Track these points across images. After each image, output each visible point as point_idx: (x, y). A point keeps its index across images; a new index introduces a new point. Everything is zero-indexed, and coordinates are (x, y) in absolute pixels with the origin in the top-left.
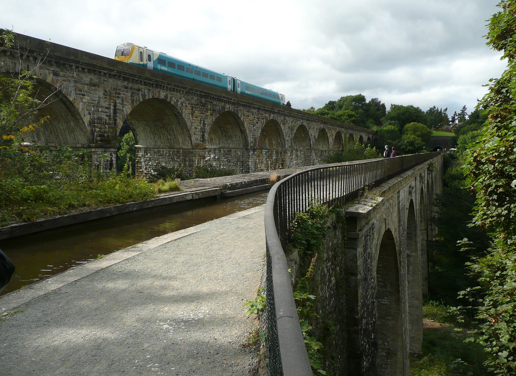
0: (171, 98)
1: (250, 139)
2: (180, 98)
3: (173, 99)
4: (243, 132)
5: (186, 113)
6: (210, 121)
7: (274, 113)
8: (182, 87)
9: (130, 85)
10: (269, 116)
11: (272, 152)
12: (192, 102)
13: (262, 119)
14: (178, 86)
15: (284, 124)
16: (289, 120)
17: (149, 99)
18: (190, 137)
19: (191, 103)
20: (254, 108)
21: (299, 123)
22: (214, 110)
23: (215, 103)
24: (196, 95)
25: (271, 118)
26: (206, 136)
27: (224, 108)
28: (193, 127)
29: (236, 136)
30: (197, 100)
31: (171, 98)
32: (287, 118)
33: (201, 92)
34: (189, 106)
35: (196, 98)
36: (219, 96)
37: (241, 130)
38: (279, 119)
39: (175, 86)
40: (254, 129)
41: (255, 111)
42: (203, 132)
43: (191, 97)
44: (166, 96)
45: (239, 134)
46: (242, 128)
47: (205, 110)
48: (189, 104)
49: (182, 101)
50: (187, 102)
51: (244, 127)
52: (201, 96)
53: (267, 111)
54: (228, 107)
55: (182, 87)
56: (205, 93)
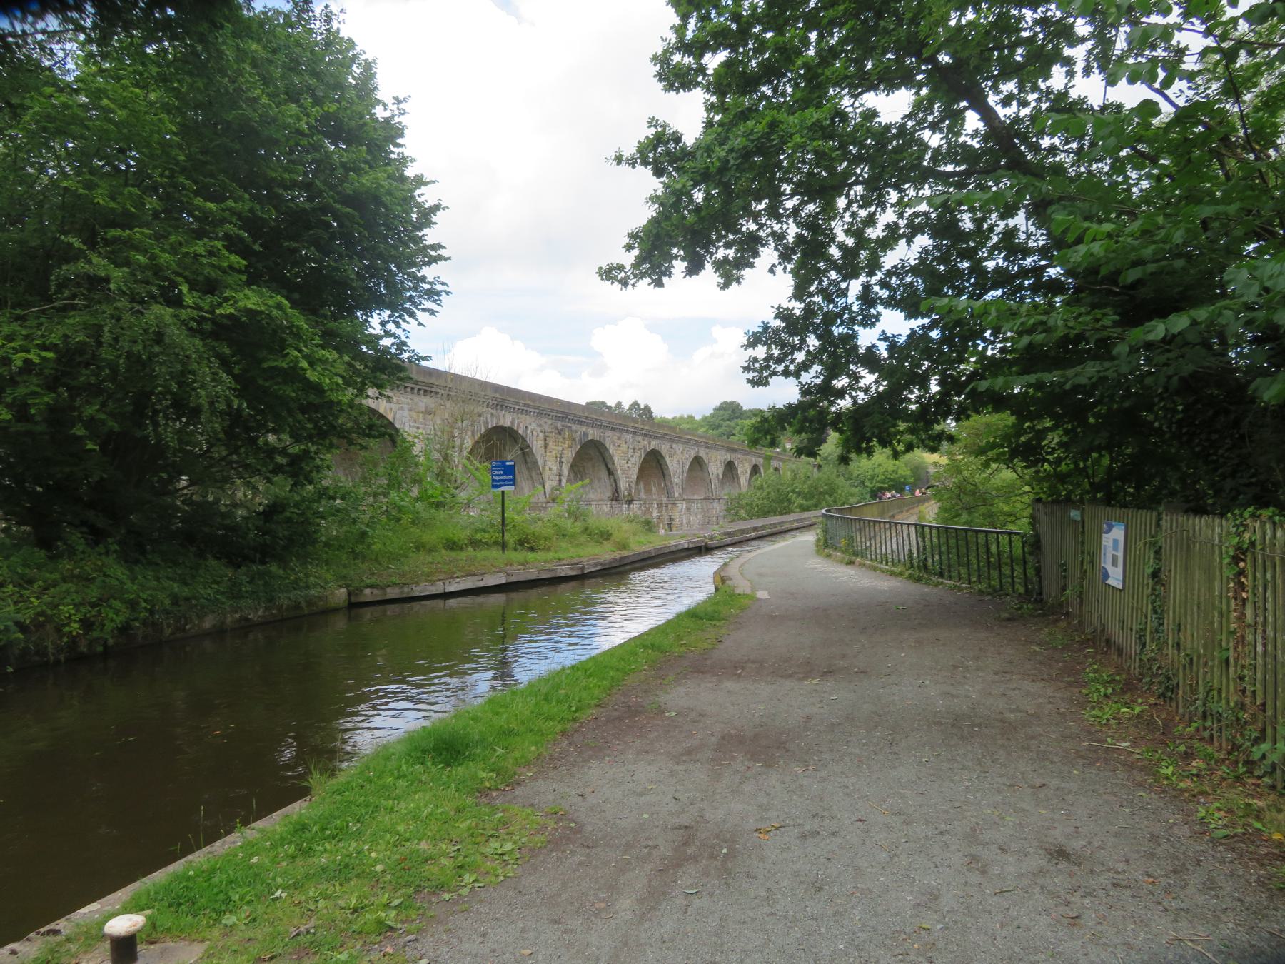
0: (519, 424)
1: (623, 484)
4: (610, 472)
5: (537, 445)
6: (569, 455)
7: (656, 437)
8: (535, 407)
10: (649, 444)
11: (651, 505)
13: (640, 449)
14: (528, 406)
15: (671, 456)
16: (678, 448)
17: (493, 428)
18: (543, 484)
20: (627, 432)
21: (693, 454)
22: (574, 440)
23: (574, 427)
25: (652, 447)
26: (564, 481)
27: (585, 434)
28: (547, 468)
29: (599, 480)
31: (519, 424)
32: (674, 446)
33: (557, 412)
35: (550, 422)
36: (581, 417)
37: (609, 470)
38: (664, 448)
39: (525, 405)
41: (628, 437)
42: (560, 475)
43: (542, 422)
44: (512, 422)
45: (604, 474)
46: (610, 466)
50: (539, 429)
51: (613, 464)
52: (558, 418)
53: (646, 435)
54: (593, 434)
55: (535, 407)
56: (562, 413)
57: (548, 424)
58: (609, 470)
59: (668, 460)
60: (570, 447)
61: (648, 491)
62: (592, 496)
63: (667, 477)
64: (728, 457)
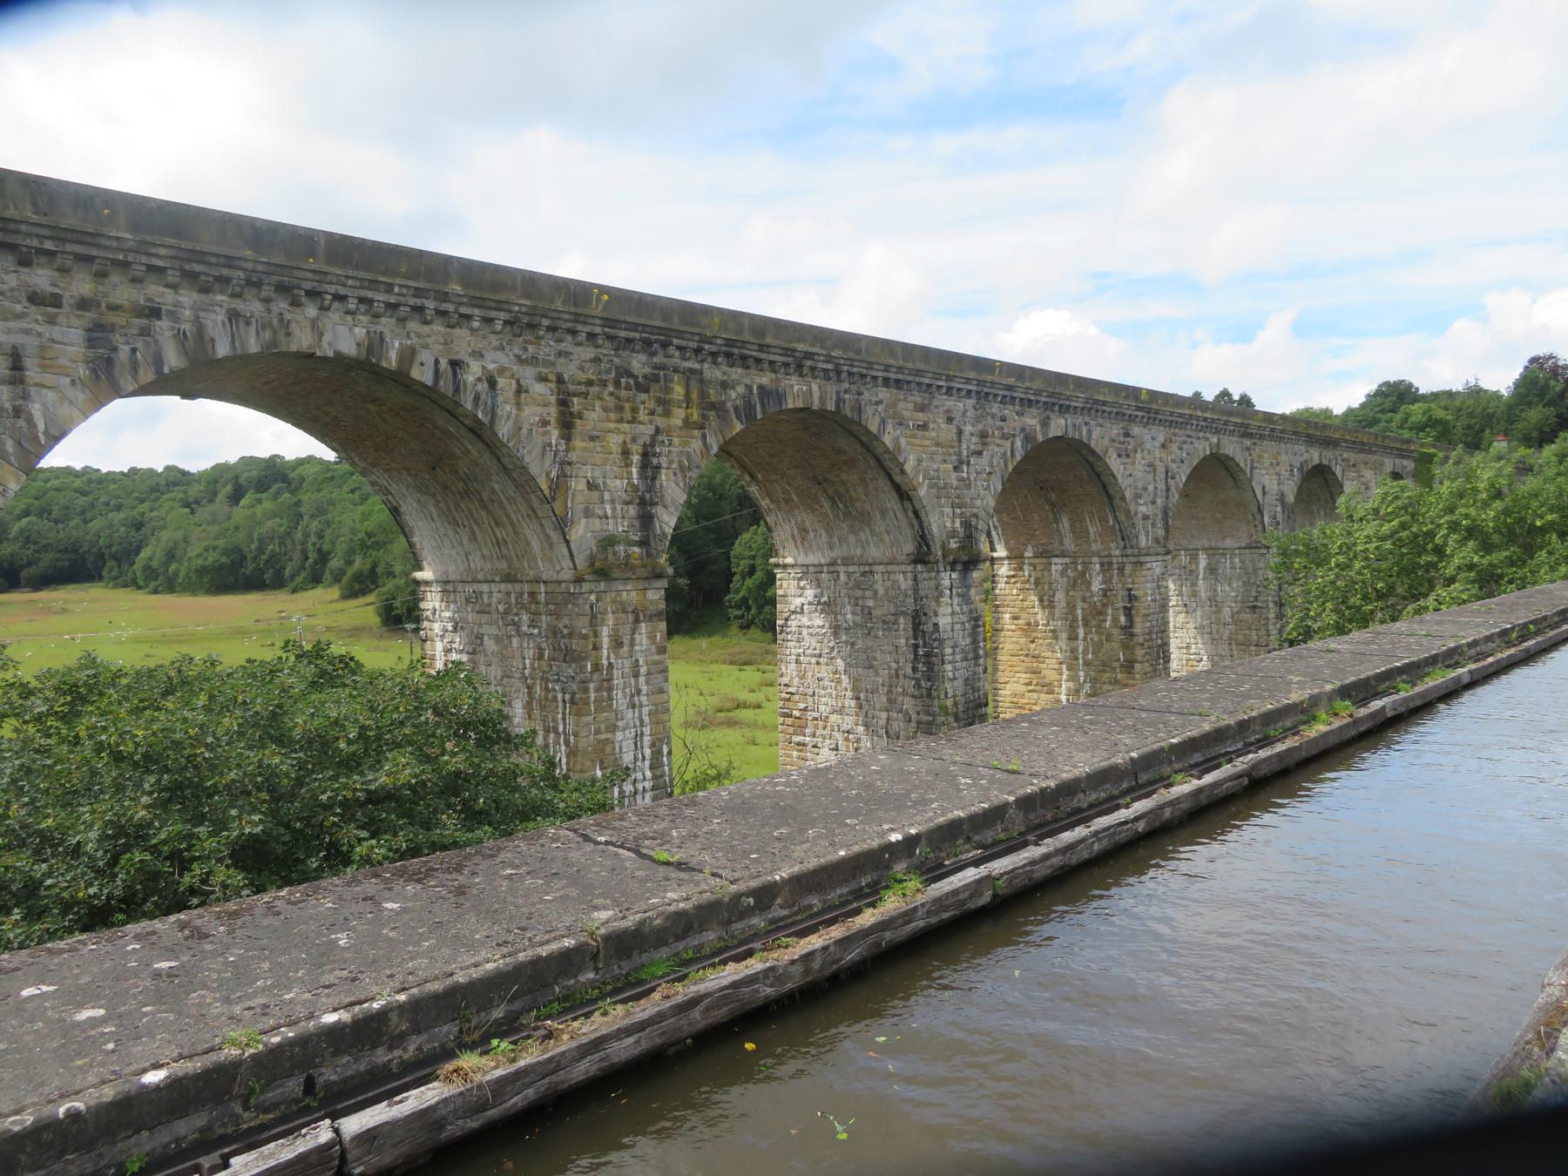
2: (478, 355)
3: (426, 356)
9: (83, 285)
12: (559, 369)
19: (553, 377)
24: (582, 337)
30: (596, 360)
33: (609, 322)
34: (539, 389)
37: (897, 488)
40: (962, 480)
43: (547, 348)
47: (652, 404)
48: (543, 379)
49: (491, 367)
50: (527, 374)
57: (578, 361)
58: (897, 488)
59: (1115, 463)
60: (687, 423)
61: (1080, 534)
62: (874, 552)
63: (1117, 502)
64: (1315, 456)
